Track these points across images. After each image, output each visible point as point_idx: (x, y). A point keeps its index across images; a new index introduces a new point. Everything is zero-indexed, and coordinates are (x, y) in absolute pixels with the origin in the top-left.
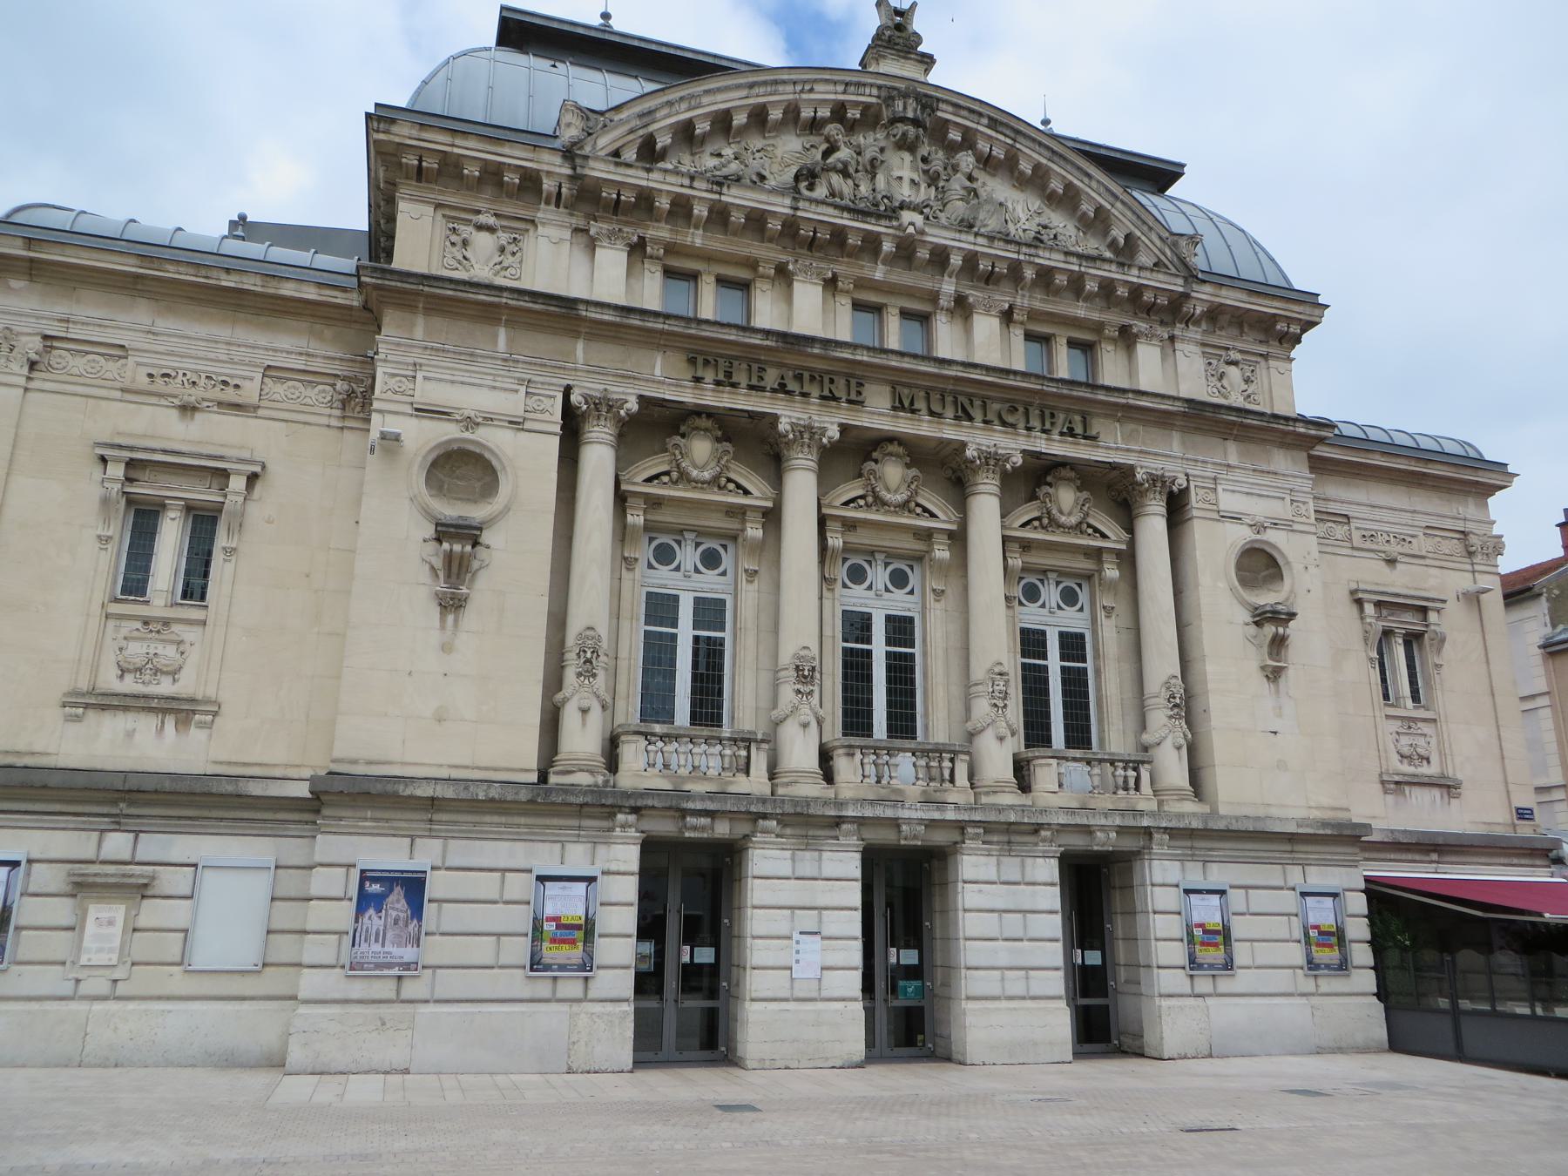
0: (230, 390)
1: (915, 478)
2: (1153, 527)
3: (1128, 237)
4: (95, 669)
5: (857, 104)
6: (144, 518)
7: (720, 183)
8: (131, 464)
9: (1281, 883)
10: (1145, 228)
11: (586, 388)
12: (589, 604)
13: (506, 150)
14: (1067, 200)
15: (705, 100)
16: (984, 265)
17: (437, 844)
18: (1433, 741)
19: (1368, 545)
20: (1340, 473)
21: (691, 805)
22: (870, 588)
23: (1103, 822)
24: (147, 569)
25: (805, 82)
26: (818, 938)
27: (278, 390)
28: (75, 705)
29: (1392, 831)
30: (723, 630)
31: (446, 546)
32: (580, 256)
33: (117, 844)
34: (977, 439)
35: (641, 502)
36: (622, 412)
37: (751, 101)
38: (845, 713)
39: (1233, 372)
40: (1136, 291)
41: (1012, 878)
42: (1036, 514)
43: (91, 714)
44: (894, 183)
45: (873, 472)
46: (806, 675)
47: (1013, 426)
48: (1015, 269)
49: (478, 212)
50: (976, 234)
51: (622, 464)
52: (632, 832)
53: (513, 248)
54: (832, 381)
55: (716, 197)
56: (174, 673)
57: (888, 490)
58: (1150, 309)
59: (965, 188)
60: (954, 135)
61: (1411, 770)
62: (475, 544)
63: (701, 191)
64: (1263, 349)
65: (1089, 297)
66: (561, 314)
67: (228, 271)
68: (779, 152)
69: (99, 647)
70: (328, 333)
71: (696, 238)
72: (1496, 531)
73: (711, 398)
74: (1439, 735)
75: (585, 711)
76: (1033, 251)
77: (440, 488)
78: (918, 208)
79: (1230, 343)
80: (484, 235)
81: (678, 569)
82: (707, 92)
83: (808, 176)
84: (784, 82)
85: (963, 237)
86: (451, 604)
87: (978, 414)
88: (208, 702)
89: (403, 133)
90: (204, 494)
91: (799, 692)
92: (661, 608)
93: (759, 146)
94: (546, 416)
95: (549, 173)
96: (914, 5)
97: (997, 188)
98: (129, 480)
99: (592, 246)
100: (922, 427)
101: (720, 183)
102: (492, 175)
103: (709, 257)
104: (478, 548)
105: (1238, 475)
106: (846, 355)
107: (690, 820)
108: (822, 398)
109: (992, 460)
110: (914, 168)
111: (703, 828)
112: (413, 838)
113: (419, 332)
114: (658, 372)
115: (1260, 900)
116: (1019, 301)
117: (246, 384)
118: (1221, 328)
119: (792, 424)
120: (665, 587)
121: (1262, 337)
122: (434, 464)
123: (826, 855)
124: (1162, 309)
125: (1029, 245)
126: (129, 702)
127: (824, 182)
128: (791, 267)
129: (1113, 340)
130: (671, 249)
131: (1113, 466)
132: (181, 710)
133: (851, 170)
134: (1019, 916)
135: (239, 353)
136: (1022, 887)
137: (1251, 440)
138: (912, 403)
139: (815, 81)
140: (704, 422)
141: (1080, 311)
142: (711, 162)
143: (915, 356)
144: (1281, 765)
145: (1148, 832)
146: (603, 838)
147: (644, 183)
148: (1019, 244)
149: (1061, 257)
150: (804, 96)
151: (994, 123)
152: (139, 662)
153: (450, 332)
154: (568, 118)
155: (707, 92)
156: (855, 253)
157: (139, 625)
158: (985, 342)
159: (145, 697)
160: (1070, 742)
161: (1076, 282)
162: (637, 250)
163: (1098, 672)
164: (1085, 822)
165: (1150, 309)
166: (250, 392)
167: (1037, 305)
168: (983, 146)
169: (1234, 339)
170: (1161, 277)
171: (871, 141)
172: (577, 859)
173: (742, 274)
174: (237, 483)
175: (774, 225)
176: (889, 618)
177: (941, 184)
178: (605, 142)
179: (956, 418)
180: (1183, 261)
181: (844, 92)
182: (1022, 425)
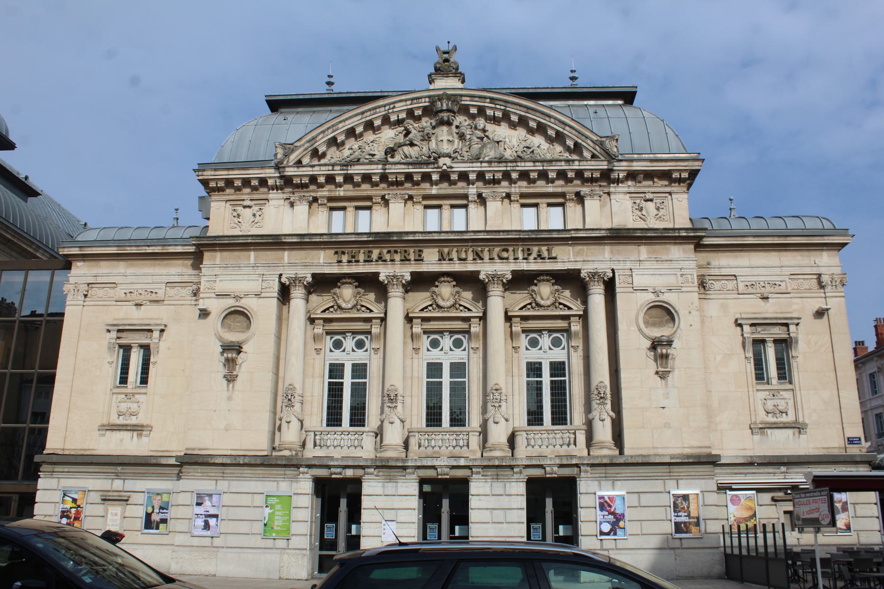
0: (154, 295)
1: (458, 292)
2: (597, 299)
5: (419, 108)
8: (119, 331)
9: (662, 490)
10: (583, 138)
11: (288, 273)
12: (293, 374)
13: (251, 172)
14: (541, 129)
15: (340, 125)
16: (488, 176)
17: (226, 483)
18: (791, 402)
19: (750, 290)
21: (332, 463)
22: (442, 350)
23: (549, 462)
26: (394, 523)
27: (171, 292)
28: (102, 430)
29: (751, 457)
30: (365, 378)
31: (225, 355)
33: (118, 484)
34: (485, 269)
35: (321, 321)
37: (363, 120)
38: (428, 414)
40: (579, 174)
41: (498, 493)
43: (108, 433)
47: (507, 259)
48: (507, 175)
50: (481, 162)
52: (308, 476)
53: (259, 213)
54: (405, 251)
57: (443, 300)
58: (592, 180)
60: (473, 111)
61: (774, 420)
62: (239, 352)
63: (337, 170)
64: (668, 189)
66: (274, 243)
67: (148, 246)
68: (382, 140)
69: (110, 406)
73: (346, 269)
75: (288, 422)
76: (514, 164)
77: (230, 328)
80: (247, 209)
81: (344, 351)
82: (341, 122)
83: (391, 151)
84: (379, 107)
85: (474, 165)
86: (230, 379)
87: (486, 255)
88: (148, 426)
89: (208, 174)
90: (143, 339)
94: (271, 290)
95: (270, 177)
96: (455, 48)
97: (501, 131)
99: (292, 205)
100: (457, 267)
102: (246, 182)
105: (647, 265)
107: (333, 470)
108: (402, 260)
109: (494, 277)
111: (340, 474)
112: (217, 480)
113: (218, 261)
114: (321, 261)
115: (646, 499)
116: (513, 190)
118: (640, 182)
119: (387, 277)
121: (666, 183)
123: (399, 484)
125: (511, 162)
126: (120, 428)
127: (401, 152)
128: (387, 197)
130: (330, 199)
132: (138, 429)
133: (415, 142)
134: (501, 512)
135: (157, 279)
136: (504, 497)
141: (550, 189)
143: (447, 232)
144: (667, 425)
145: (577, 465)
146: (295, 478)
147: (311, 173)
148: (506, 161)
149: (532, 164)
151: (492, 100)
155: (341, 122)
157: (123, 396)
159: (127, 425)
160: (555, 422)
161: (543, 175)
164: (538, 463)
166: (161, 295)
167: (525, 190)
168: (489, 112)
170: (593, 163)
172: (284, 487)
173: (368, 204)
174: (156, 334)
175: (376, 179)
176: (451, 364)
177: (468, 137)
178: (293, 157)
182: (511, 257)
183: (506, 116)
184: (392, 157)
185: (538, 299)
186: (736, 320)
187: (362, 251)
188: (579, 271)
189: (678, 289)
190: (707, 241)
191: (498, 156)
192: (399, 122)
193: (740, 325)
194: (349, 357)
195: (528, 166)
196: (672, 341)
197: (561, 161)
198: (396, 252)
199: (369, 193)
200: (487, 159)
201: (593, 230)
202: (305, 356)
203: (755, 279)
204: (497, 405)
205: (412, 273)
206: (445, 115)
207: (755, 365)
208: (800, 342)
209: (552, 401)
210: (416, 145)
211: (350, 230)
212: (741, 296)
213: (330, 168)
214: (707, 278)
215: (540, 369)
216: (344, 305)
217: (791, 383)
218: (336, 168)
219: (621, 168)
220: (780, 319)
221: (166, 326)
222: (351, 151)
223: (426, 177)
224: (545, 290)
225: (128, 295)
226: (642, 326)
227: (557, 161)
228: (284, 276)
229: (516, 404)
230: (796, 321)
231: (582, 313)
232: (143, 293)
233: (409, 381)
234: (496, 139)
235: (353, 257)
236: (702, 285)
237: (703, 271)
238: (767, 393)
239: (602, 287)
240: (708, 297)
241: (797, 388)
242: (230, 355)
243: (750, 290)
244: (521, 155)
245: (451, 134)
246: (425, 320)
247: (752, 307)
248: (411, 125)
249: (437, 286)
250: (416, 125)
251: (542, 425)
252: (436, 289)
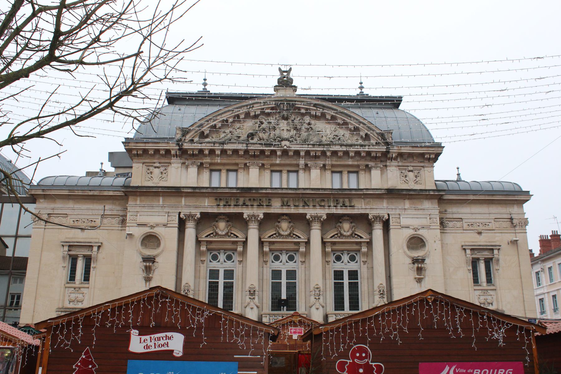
0: (93, 222)
1: (292, 226)
2: (378, 232)
3: (366, 135)
4: (63, 301)
6: (74, 260)
7: (223, 143)
8: (70, 246)
11: (185, 211)
13: (160, 145)
18: (495, 297)
20: (456, 203)
22: (281, 262)
24: (75, 274)
25: (250, 105)
28: (59, 311)
30: (233, 279)
32: (184, 170)
34: (310, 212)
37: (233, 114)
39: (411, 175)
40: (369, 153)
42: (336, 233)
44: (282, 132)
45: (278, 226)
46: (252, 293)
47: (324, 206)
48: (324, 153)
49: (154, 163)
50: (308, 145)
54: (260, 200)
56: (82, 302)
57: (283, 231)
58: (376, 158)
60: (303, 111)
62: (154, 262)
65: (352, 157)
66: (176, 192)
67: (90, 190)
68: (245, 127)
69: (64, 296)
70: (117, 203)
71: (218, 160)
72: (526, 217)
73: (222, 210)
74: (497, 294)
77: (146, 246)
78: (287, 140)
79: (409, 164)
80: (157, 169)
81: (219, 261)
82: (219, 115)
83: (251, 136)
84: (244, 106)
85: (304, 146)
89: (132, 146)
90: (88, 253)
91: (250, 298)
92: (214, 274)
93: (238, 127)
94: (174, 222)
95: (173, 149)
97: (319, 125)
98: (69, 250)
99: (187, 167)
100: (292, 211)
101: (223, 143)
102: (157, 151)
103: (224, 164)
104: (155, 263)
105: (409, 212)
109: (316, 218)
110: (288, 124)
113: (138, 202)
116: (327, 162)
117: (97, 220)
118: (405, 160)
119: (248, 215)
120: (215, 267)
121: (422, 160)
122: (143, 239)
124: (379, 157)
129: (365, 170)
130: (211, 164)
131: (361, 215)
137: (414, 199)
138: (287, 203)
140: (222, 217)
141: (350, 162)
142: (223, 135)
148: (324, 145)
149: (339, 147)
150: (251, 109)
152: (73, 299)
153: (147, 201)
154: (178, 132)
155: (219, 115)
156: (268, 156)
157: (73, 289)
158: (315, 179)
161: (346, 153)
162: (201, 166)
163: (361, 283)
165: (376, 158)
167: (334, 163)
168: (313, 113)
169: (411, 162)
171: (272, 120)
174: (95, 249)
175: (241, 153)
176: (288, 271)
179: (304, 206)
181: (264, 105)
182: (327, 205)
183: (323, 115)
185: (342, 232)
186: (462, 246)
187: (232, 198)
188: (368, 215)
189: (428, 227)
190: (446, 197)
192: (256, 117)
193: (465, 249)
194: (222, 265)
196: (425, 260)
197: (357, 145)
198: (254, 200)
199: (237, 161)
200: (312, 143)
201: (377, 189)
202: (195, 264)
203: (473, 221)
204: (317, 298)
205: (264, 214)
207: (473, 274)
208: (500, 261)
209: (350, 295)
211: (223, 185)
212: (465, 231)
213: (212, 145)
214: (445, 220)
215: (343, 275)
217: (493, 285)
219: (394, 150)
220: (489, 246)
221: (102, 243)
222: (225, 134)
223: (273, 152)
224: (346, 226)
225: (76, 222)
226: (406, 250)
227: (355, 145)
229: (328, 297)
230: (498, 247)
231: (368, 240)
232: (86, 221)
233: (261, 281)
234: (317, 129)
235: (227, 202)
236: (442, 223)
237: (443, 216)
238: (481, 291)
240: (445, 231)
241: (498, 289)
242: (148, 264)
243: (471, 228)
244: (333, 140)
246: (271, 243)
247: (472, 239)
248: (262, 118)
249: (279, 222)
250: (266, 118)
251: (344, 310)
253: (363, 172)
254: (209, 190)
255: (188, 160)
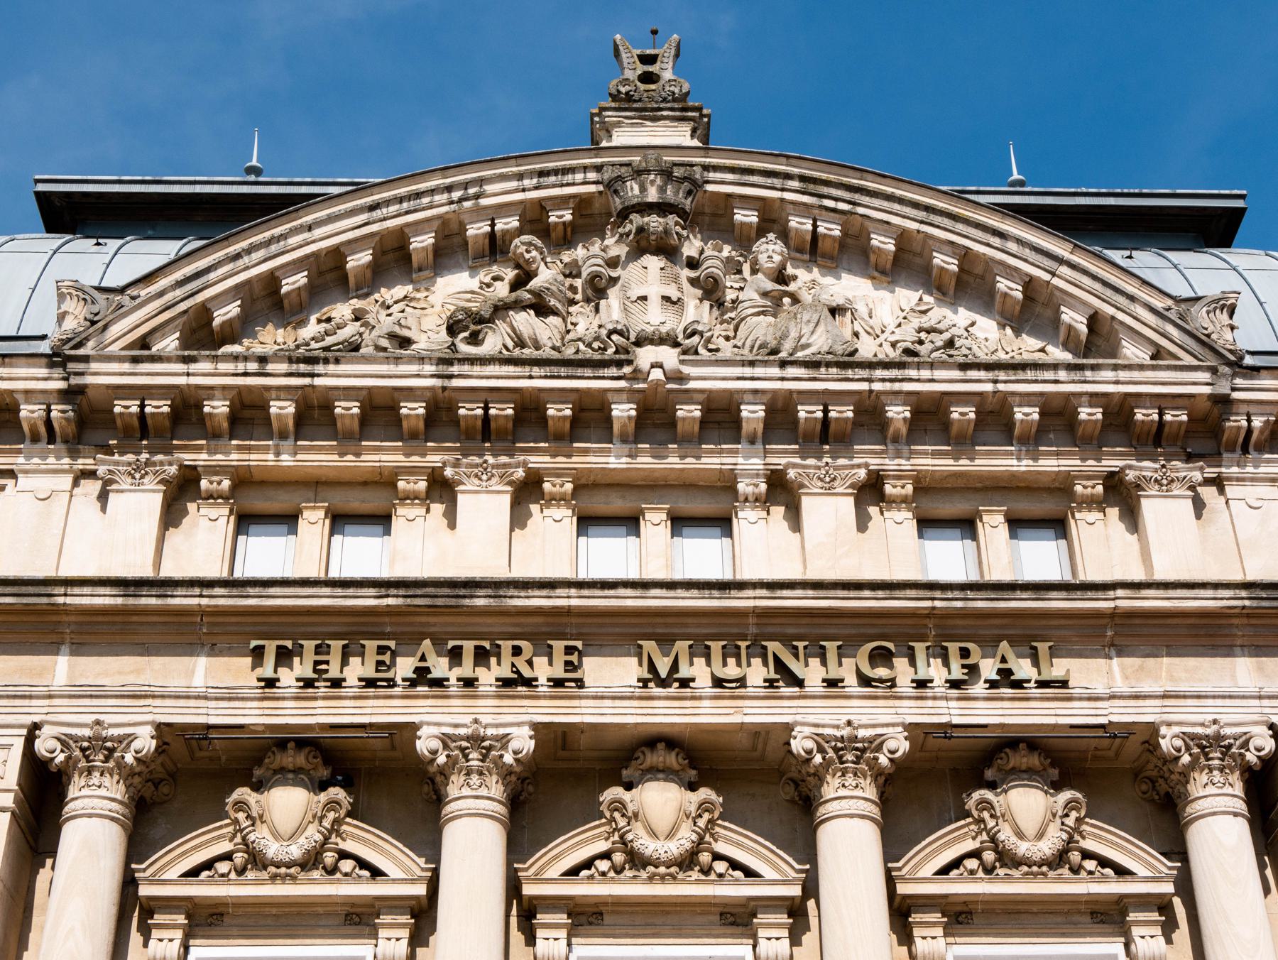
3: (1094, 320)
5: (562, 202)
25: (466, 185)
34: (812, 715)
36: (129, 758)
40: (1118, 412)
44: (634, 308)
45: (619, 806)
50: (783, 364)
51: (139, 844)
54: (517, 651)
55: (307, 381)
57: (653, 834)
59: (765, 294)
63: (279, 375)
85: (759, 371)
95: (27, 392)
106: (538, 600)
109: (853, 751)
119: (446, 740)
138: (675, 667)
139: (481, 182)
140: (291, 758)
147: (182, 381)
168: (799, 224)
177: (730, 295)
178: (122, 330)
180: (1205, 343)
184: (475, 339)
185: (1006, 834)
191: (839, 349)
192: (495, 248)
195: (945, 381)
200: (800, 355)
206: (655, 222)
210: (555, 312)
213: (253, 366)
216: (273, 849)
218: (271, 367)
228: (47, 731)
239: (1238, 789)
245: (676, 279)
252: (626, 796)
253: (1094, 516)
254: (222, 599)
255: (108, 450)
